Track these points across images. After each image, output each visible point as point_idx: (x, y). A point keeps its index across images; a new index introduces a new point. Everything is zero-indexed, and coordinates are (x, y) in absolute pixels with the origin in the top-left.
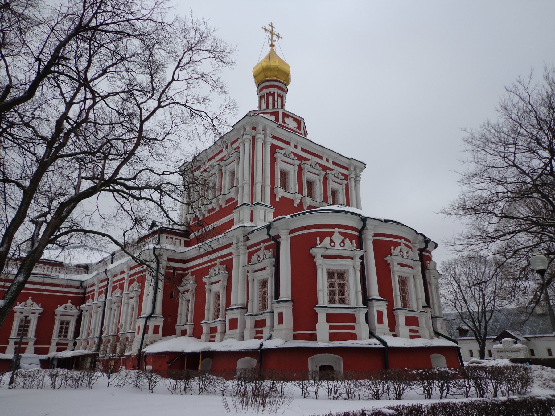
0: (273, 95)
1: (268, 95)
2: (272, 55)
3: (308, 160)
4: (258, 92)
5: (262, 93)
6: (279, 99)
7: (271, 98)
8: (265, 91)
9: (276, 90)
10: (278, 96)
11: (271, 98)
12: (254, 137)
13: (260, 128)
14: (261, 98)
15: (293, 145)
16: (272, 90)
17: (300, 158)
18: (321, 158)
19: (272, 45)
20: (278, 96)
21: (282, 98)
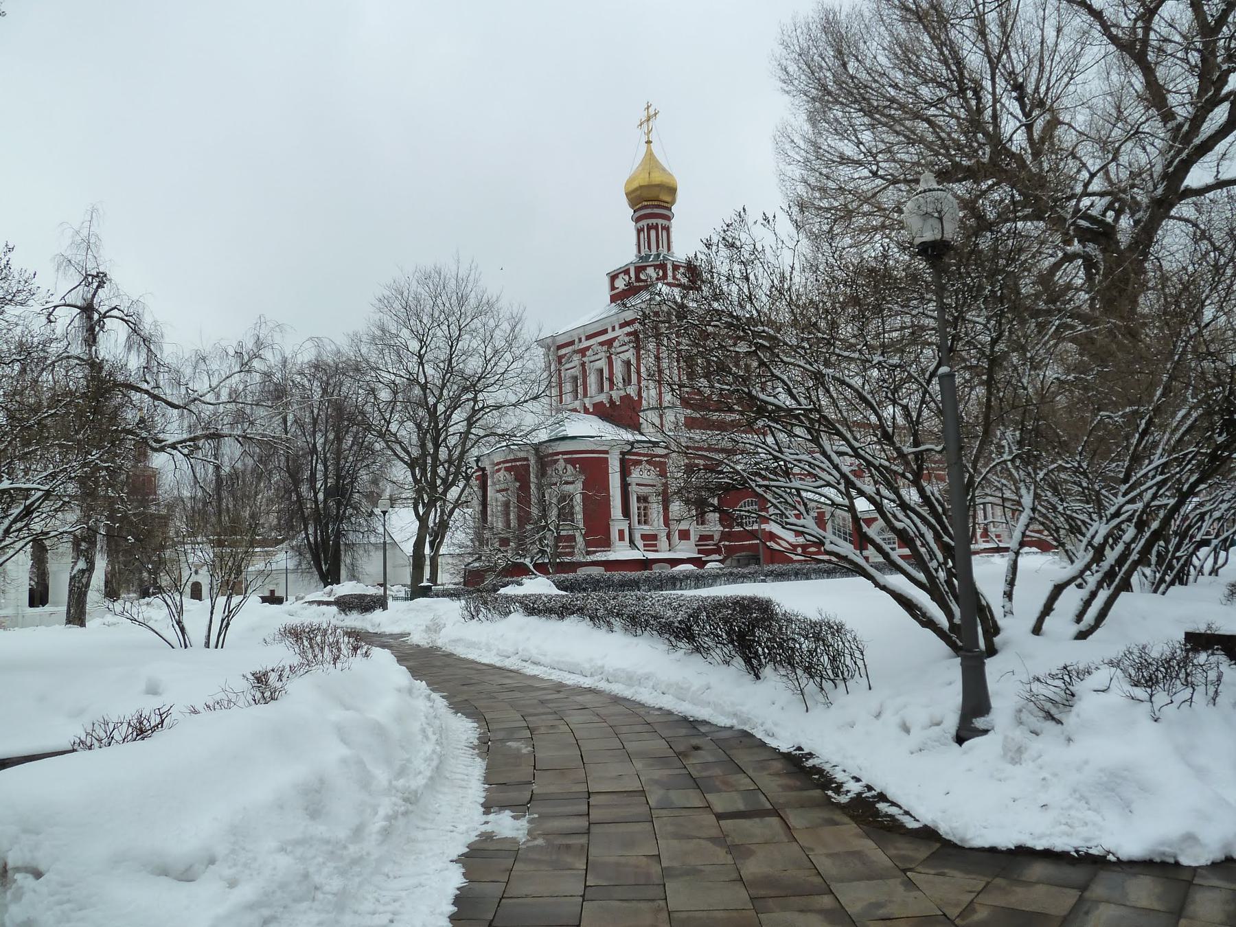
0: (656, 227)
1: (649, 228)
2: (650, 158)
4: (637, 220)
5: (640, 224)
6: (665, 233)
7: (653, 233)
8: (644, 223)
9: (660, 222)
10: (663, 228)
11: (653, 233)
14: (639, 231)
19: (649, 142)
20: (663, 228)
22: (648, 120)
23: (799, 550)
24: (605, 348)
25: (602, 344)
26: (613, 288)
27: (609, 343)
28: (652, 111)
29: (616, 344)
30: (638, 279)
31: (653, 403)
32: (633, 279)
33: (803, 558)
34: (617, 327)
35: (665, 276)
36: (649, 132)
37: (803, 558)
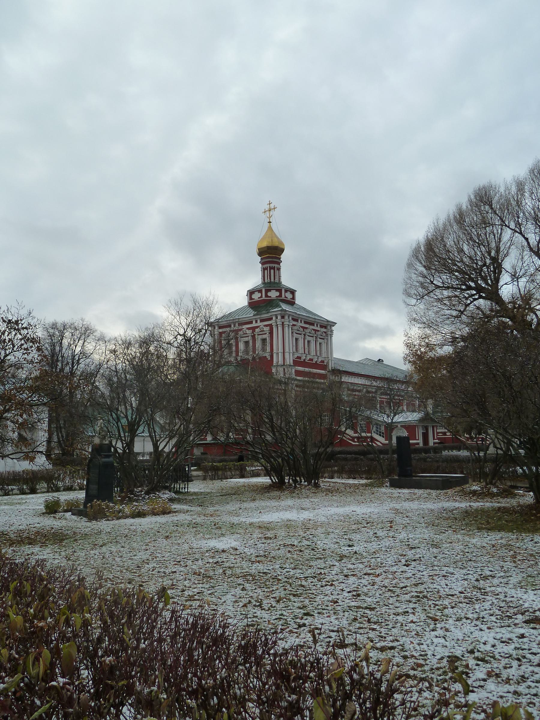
0: (274, 268)
1: (271, 268)
3: (307, 328)
4: (263, 264)
5: (266, 266)
7: (272, 271)
8: (268, 265)
9: (276, 266)
11: (272, 271)
12: (283, 323)
13: (286, 317)
14: (264, 270)
15: (299, 321)
16: (273, 265)
17: (304, 328)
18: (313, 325)
21: (279, 269)
22: (270, 210)
23: (356, 440)
24: (251, 331)
25: (248, 329)
26: (251, 298)
27: (253, 329)
28: (272, 206)
29: (257, 330)
30: (266, 296)
31: (281, 362)
32: (264, 296)
33: (357, 444)
34: (259, 321)
35: (280, 295)
36: (270, 217)
37: (357, 444)
